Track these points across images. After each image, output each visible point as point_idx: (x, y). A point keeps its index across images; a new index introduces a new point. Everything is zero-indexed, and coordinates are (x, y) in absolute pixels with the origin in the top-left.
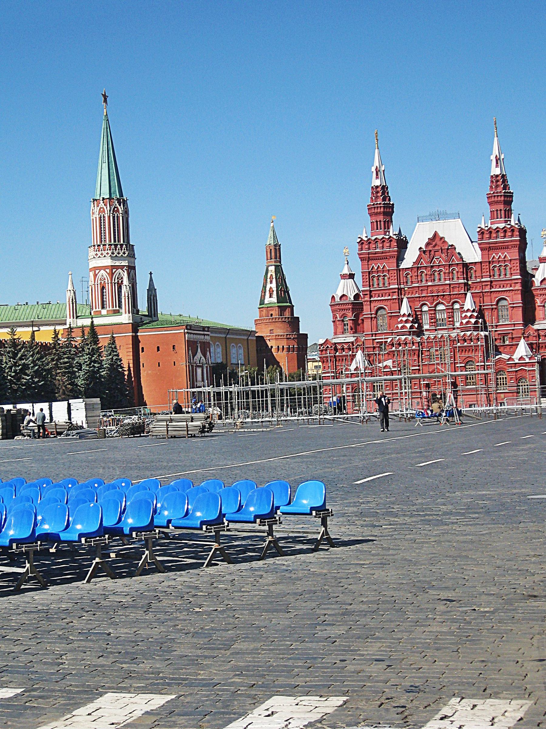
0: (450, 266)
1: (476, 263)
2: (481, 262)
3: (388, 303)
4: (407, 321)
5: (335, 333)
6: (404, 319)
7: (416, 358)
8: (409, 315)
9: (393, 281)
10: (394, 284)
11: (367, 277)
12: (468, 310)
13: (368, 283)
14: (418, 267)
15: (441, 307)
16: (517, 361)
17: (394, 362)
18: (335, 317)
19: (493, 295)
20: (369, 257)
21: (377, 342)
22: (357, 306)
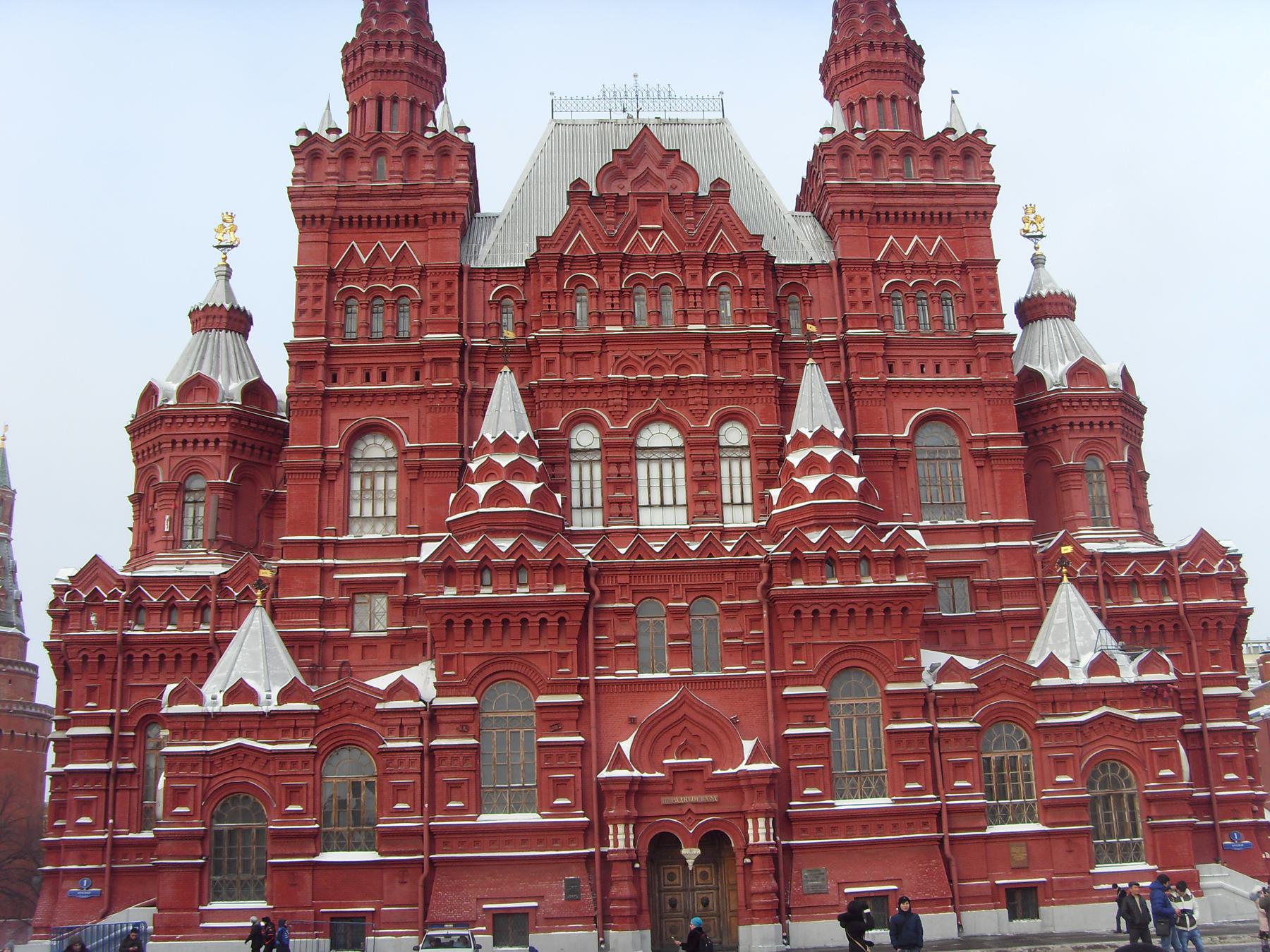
0: (709, 262)
1: (812, 267)
2: (839, 264)
3: (412, 412)
4: (519, 470)
5: (141, 552)
6: (504, 460)
7: (567, 646)
8: (526, 445)
9: (435, 317)
10: (443, 326)
11: (323, 291)
12: (823, 436)
13: (322, 318)
14: (562, 259)
15: (660, 436)
16: (1079, 677)
17: (444, 664)
18: (144, 474)
19: (899, 404)
20: (336, 208)
21: (343, 583)
22: (255, 429)
